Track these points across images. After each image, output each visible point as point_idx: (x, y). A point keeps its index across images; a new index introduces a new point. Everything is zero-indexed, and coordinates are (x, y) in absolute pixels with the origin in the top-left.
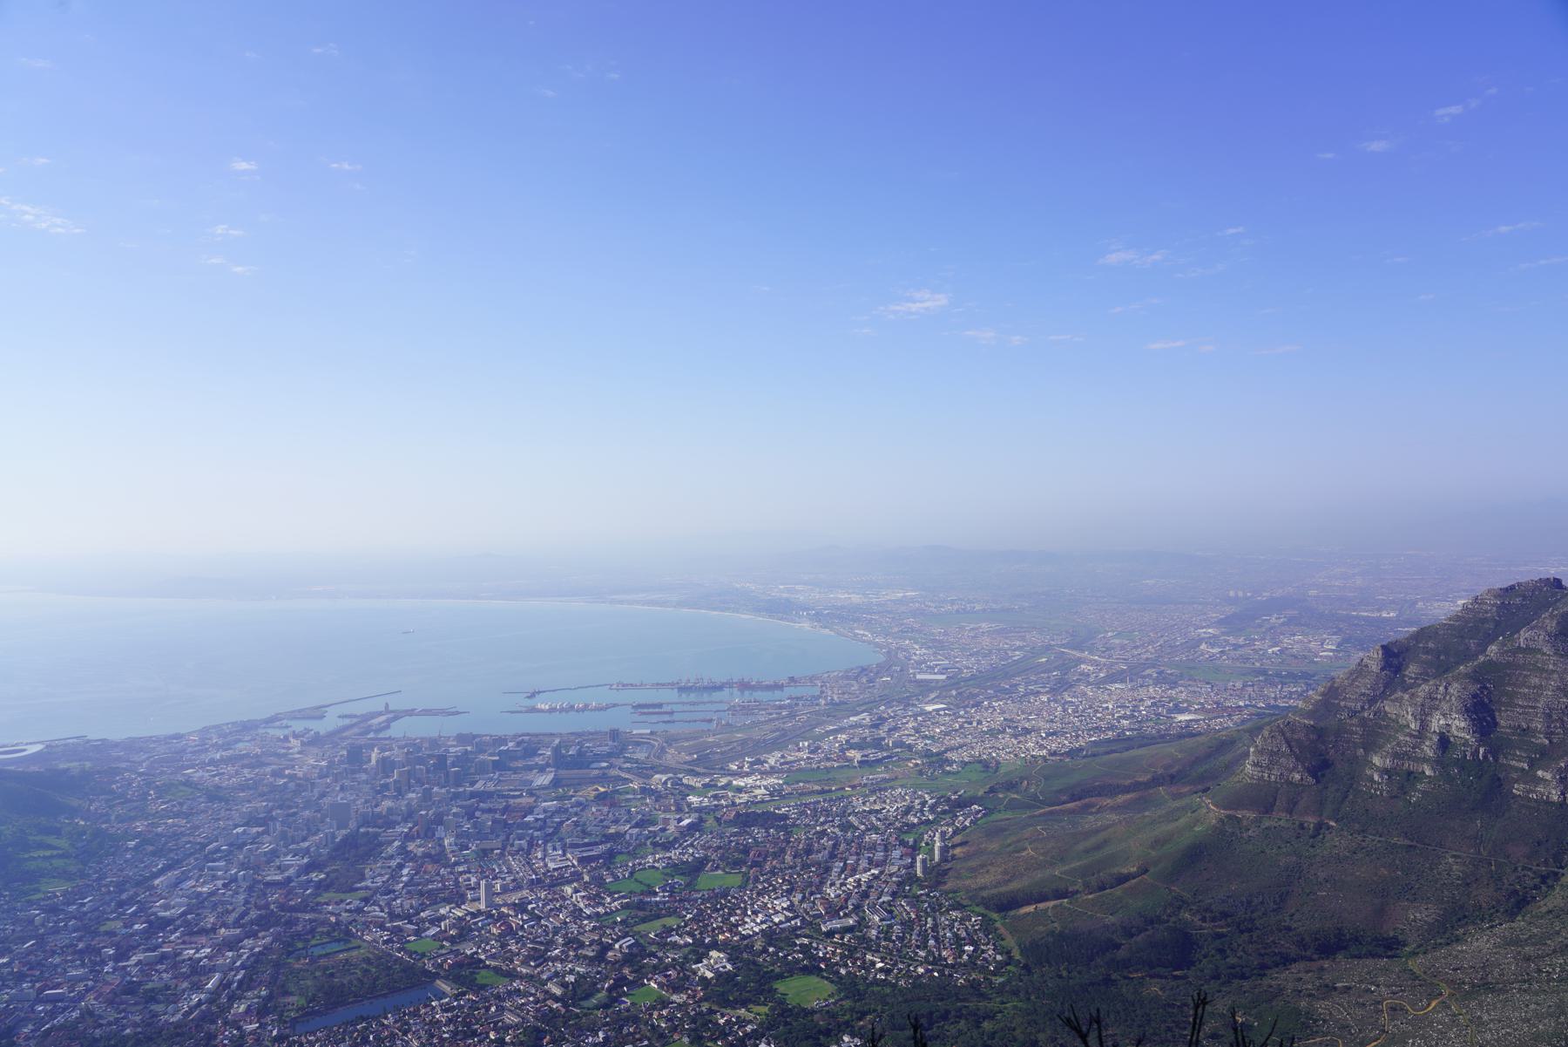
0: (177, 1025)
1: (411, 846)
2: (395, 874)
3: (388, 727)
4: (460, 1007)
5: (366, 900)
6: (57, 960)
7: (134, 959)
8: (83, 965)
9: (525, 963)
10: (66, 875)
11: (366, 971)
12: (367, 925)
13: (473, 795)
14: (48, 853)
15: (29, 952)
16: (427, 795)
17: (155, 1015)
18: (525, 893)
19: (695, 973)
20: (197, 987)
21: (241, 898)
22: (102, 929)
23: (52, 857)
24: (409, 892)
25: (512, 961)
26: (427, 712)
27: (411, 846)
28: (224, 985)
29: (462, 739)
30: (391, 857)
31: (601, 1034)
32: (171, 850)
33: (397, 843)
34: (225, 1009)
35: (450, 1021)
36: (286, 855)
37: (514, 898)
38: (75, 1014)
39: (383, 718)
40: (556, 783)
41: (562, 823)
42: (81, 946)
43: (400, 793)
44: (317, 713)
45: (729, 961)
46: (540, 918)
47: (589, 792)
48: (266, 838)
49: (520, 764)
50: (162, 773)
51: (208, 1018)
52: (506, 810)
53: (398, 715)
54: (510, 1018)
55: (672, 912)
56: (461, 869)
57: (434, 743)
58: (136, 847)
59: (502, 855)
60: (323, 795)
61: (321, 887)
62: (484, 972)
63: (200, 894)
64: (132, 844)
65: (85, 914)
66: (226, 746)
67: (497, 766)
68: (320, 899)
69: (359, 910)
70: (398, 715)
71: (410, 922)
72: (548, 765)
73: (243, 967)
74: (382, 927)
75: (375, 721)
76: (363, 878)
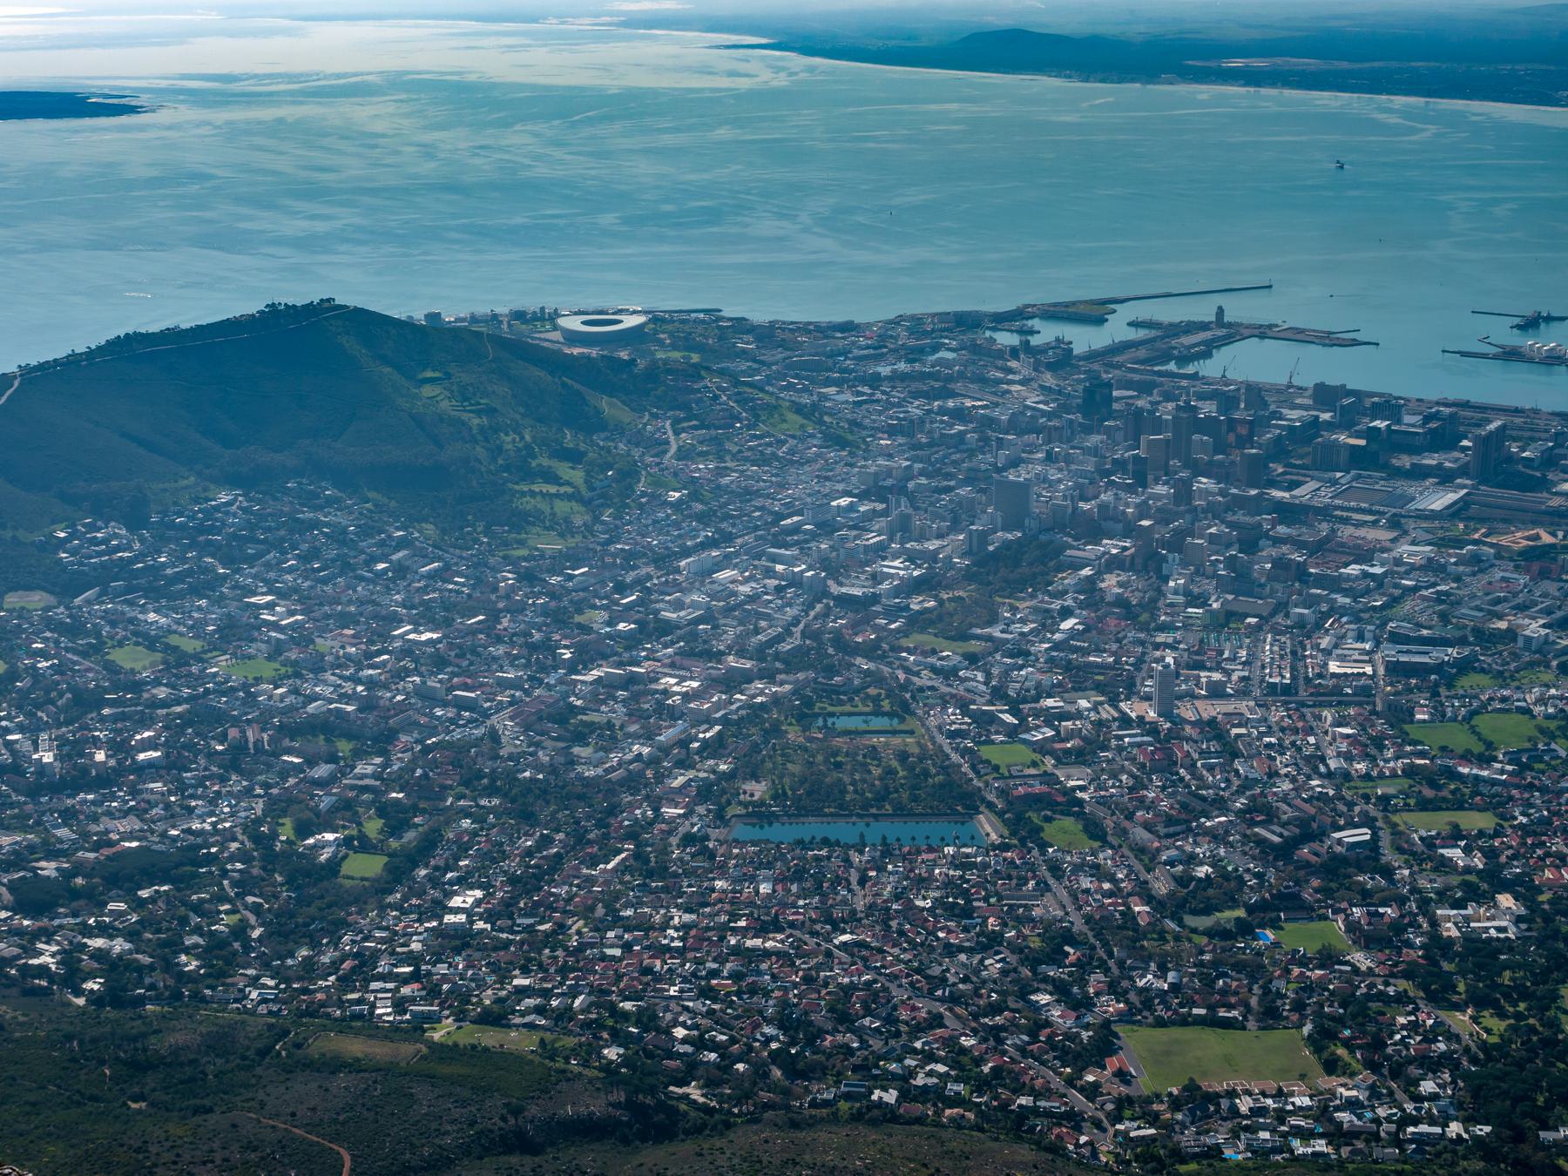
0: (588, 783)
1: (1110, 583)
2: (1048, 621)
3: (1207, 355)
6: (500, 650)
8: (526, 666)
9: (1147, 826)
10: (564, 528)
11: (890, 772)
12: (944, 702)
14: (553, 489)
15: (473, 631)
17: (572, 762)
18: (1244, 706)
19: (1434, 923)
20: (648, 736)
22: (578, 619)
23: (557, 495)
24: (1051, 661)
25: (1130, 816)
26: (1298, 336)
27: (1110, 583)
28: (684, 743)
29: (1325, 395)
30: (1061, 594)
31: (1171, 977)
32: (727, 517)
33: (1087, 572)
34: (660, 778)
35: (949, 883)
36: (895, 557)
39: (1207, 335)
40: (1455, 512)
41: (1415, 589)
42: (537, 636)
43: (1141, 481)
44: (1093, 313)
45: (1518, 920)
46: (1236, 754)
47: (1518, 539)
48: (881, 523)
49: (1405, 461)
50: (791, 387)
51: (633, 782)
52: (1318, 548)
53: (1229, 332)
55: (1497, 804)
56: (1161, 638)
57: (1255, 393)
58: (680, 500)
59: (1258, 628)
60: (1014, 463)
61: (918, 622)
62: (1068, 823)
63: (735, 594)
65: (569, 591)
66: (913, 355)
67: (1357, 459)
68: (905, 642)
69: (949, 674)
70: (1229, 332)
71: (1014, 711)
72: (1463, 471)
73: (725, 721)
75: (1187, 340)
76: (992, 620)
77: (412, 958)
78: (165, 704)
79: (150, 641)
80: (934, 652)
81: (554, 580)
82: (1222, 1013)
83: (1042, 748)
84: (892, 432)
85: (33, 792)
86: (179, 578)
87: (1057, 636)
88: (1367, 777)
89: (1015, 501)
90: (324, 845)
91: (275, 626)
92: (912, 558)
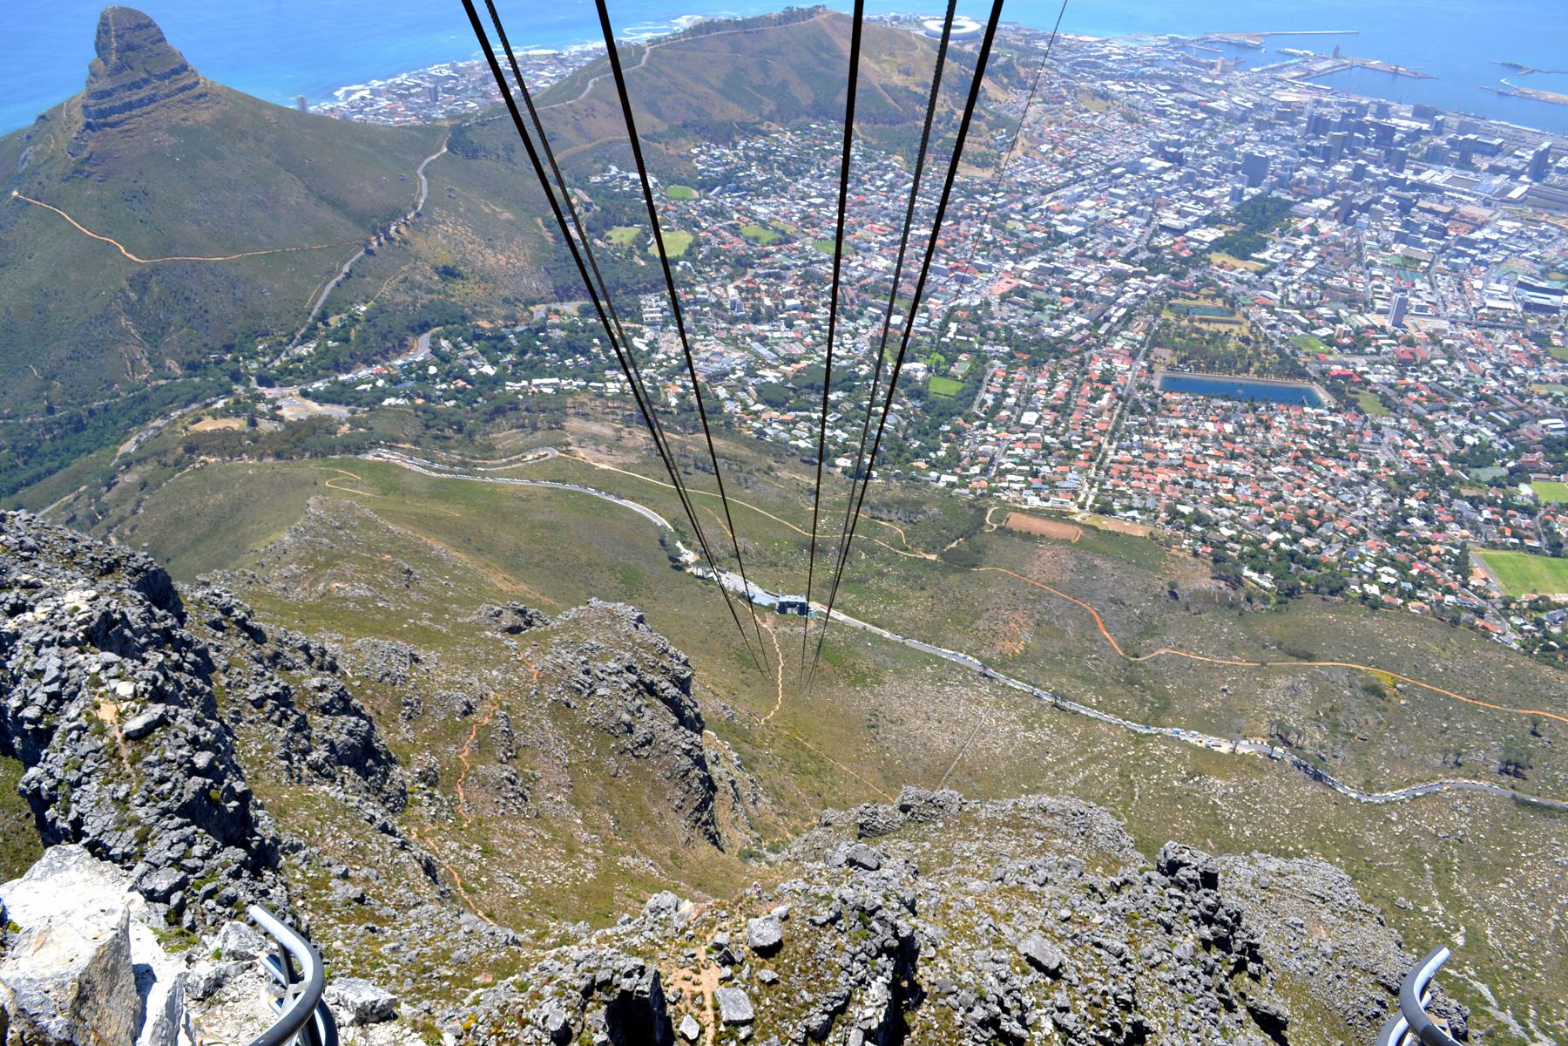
0: (1059, 340)
4: (1334, 424)
5: (1260, 274)
7: (1030, 266)
13: (1414, 186)
16: (1359, 173)
21: (1137, 231)
27: (1325, 227)
30: (1298, 234)
33: (1310, 221)
37: (1432, 324)
38: (977, 302)
52: (1447, 217)
54: (1382, 456)
61: (1217, 245)
64: (1044, 148)
72: (1522, 172)
74: (1271, 310)
76: (1263, 246)
77: (1023, 462)
78: (788, 268)
79: (764, 225)
80: (1234, 268)
81: (985, 199)
82: (1528, 542)
83: (1329, 341)
84: (1161, 113)
85: (734, 321)
86: (765, 183)
87: (1311, 264)
88: (1539, 382)
89: (1254, 168)
90: (916, 371)
91: (830, 218)
92: (1198, 200)
